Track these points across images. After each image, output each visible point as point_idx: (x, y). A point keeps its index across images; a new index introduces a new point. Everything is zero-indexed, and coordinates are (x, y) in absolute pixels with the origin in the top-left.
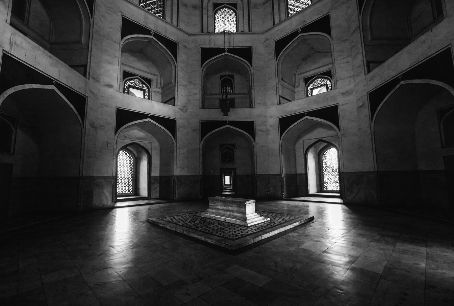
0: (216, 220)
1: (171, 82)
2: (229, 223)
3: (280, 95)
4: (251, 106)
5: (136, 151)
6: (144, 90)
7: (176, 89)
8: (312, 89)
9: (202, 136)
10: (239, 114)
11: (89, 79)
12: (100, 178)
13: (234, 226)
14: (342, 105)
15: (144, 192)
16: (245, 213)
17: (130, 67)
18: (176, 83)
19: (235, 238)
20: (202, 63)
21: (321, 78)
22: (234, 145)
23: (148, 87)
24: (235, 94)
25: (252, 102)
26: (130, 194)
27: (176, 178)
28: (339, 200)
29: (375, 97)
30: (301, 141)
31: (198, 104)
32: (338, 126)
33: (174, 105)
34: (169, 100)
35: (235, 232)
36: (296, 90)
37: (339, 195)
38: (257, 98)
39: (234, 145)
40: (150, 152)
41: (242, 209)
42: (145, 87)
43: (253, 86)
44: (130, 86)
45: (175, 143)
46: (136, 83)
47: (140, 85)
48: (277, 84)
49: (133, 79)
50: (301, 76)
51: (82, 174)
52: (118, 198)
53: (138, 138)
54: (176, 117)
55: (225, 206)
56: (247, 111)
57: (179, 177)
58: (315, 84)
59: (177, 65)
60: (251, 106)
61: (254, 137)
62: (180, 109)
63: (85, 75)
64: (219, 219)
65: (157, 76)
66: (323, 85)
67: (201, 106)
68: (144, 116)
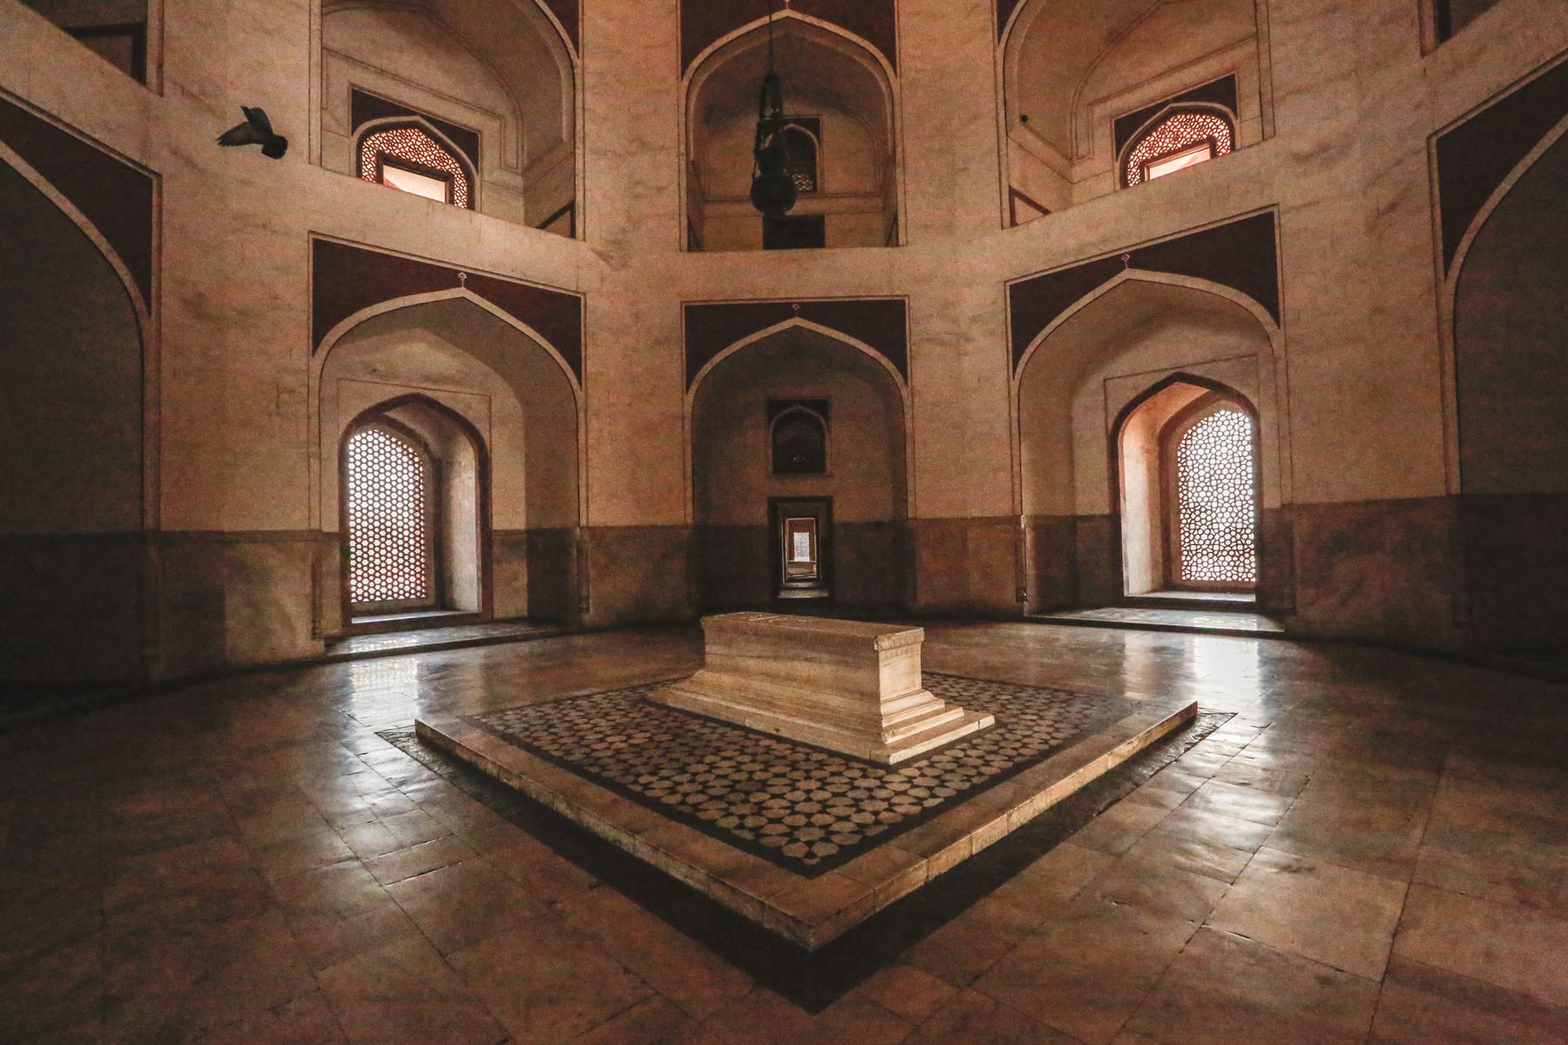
0: (735, 727)
1: (559, 140)
2: (795, 745)
3: (1016, 186)
4: (891, 238)
5: (429, 426)
6: (446, 177)
7: (579, 166)
8: (1144, 165)
9: (694, 361)
10: (845, 270)
11: (161, 95)
12: (253, 537)
13: (821, 765)
14: (1298, 208)
15: (468, 595)
16: (874, 697)
17: (382, 72)
18: (579, 145)
19: (822, 850)
20: (687, 57)
21: (1185, 111)
22: (822, 406)
23: (464, 167)
24: (824, 196)
25: (896, 220)
26: (420, 603)
27: (586, 537)
28: (1250, 623)
29: (1468, 158)
30: (1094, 383)
31: (675, 231)
32: (1273, 308)
33: (573, 235)
34: (559, 216)
35: (825, 807)
36: (1078, 171)
37: (1251, 598)
38: (915, 203)
39: (822, 406)
40: (486, 436)
41: (861, 676)
42: (451, 166)
43: (899, 156)
44: (384, 159)
45: (580, 395)
46: (412, 144)
47: (431, 156)
48: (1003, 140)
49: (396, 126)
50: (1099, 111)
51: (157, 519)
52: (355, 621)
53: (427, 378)
54: (584, 287)
55: (776, 658)
56: (879, 255)
57: (593, 530)
58: (1160, 140)
59: (577, 62)
60: (891, 238)
61: (902, 364)
62: (599, 254)
63: (139, 74)
64: (748, 723)
65: (499, 117)
66: (1196, 144)
67: (685, 241)
68: (441, 276)
